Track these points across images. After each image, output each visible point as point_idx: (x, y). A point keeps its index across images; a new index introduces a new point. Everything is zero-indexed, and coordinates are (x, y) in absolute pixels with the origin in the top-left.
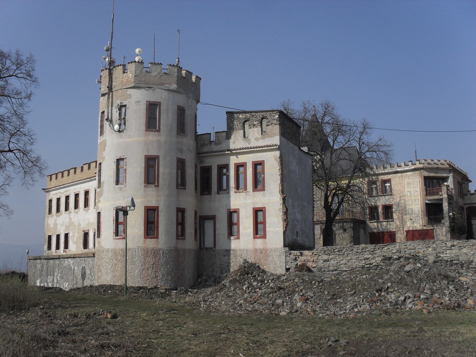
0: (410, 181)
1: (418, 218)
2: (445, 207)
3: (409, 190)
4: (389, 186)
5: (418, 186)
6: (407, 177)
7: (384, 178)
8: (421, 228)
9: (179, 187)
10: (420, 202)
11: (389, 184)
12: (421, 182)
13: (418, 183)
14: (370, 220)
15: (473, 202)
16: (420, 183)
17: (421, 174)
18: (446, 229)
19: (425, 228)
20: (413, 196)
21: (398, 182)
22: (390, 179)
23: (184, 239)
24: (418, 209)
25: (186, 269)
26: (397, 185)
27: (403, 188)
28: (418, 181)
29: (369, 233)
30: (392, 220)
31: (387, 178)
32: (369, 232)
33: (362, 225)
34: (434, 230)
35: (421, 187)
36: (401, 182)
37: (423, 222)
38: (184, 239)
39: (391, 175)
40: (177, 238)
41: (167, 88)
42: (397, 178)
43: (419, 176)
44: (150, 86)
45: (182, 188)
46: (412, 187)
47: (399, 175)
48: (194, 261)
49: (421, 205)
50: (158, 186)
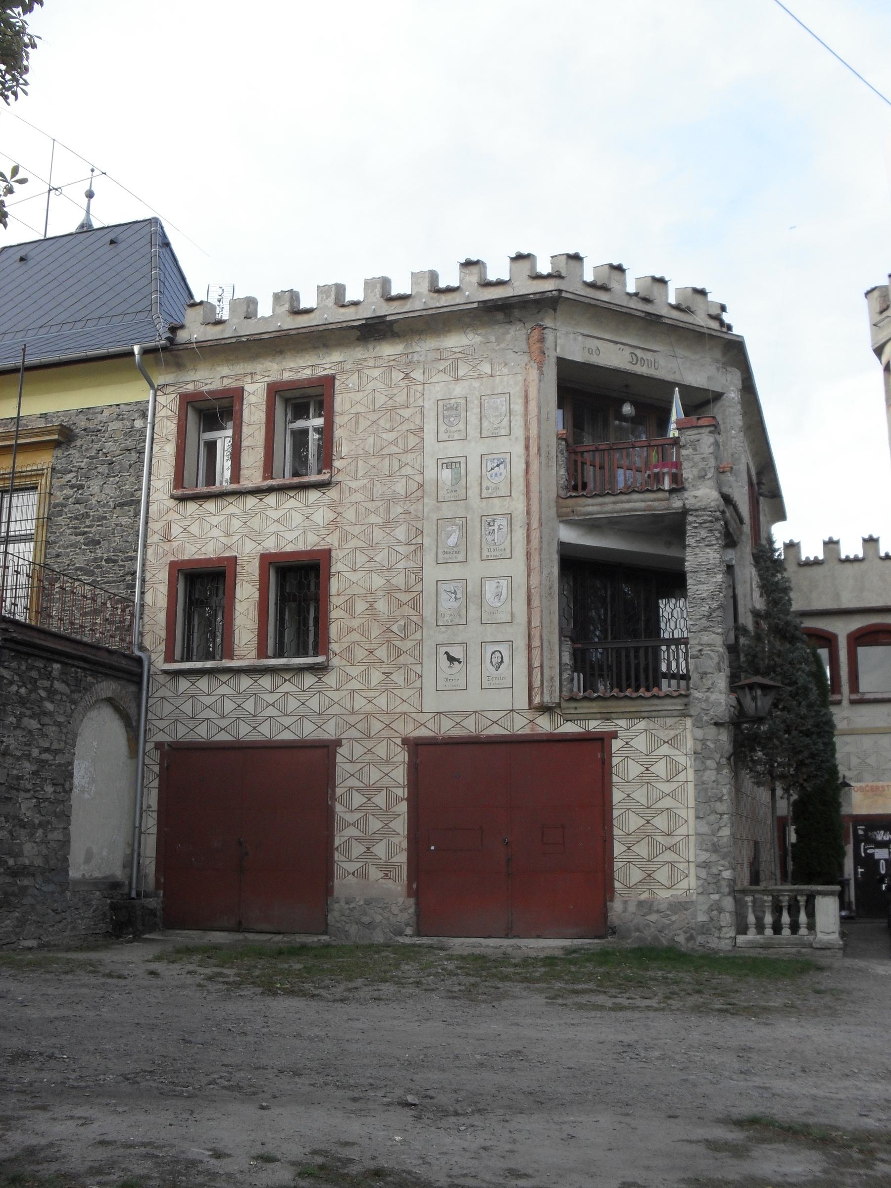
0: (459, 390)
1: (504, 649)
2: (703, 577)
3: (453, 450)
4: (317, 430)
5: (518, 422)
6: (442, 365)
7: (287, 376)
8: (520, 726)
10: (519, 535)
11: (319, 422)
12: (533, 393)
13: (518, 407)
15: (819, 604)
16: (533, 405)
17: (542, 340)
18: (699, 733)
19: (545, 725)
20: (473, 492)
21: (381, 400)
22: (330, 381)
24: (504, 583)
26: (373, 417)
27: (413, 441)
28: (516, 391)
29: (159, 746)
30: (321, 659)
31: (307, 373)
33: (107, 688)
34: (616, 744)
35: (534, 432)
36: (401, 399)
37: (537, 683)
39: (336, 356)
42: (376, 373)
43: (526, 358)
46: (473, 432)
47: (389, 350)
49: (528, 555)
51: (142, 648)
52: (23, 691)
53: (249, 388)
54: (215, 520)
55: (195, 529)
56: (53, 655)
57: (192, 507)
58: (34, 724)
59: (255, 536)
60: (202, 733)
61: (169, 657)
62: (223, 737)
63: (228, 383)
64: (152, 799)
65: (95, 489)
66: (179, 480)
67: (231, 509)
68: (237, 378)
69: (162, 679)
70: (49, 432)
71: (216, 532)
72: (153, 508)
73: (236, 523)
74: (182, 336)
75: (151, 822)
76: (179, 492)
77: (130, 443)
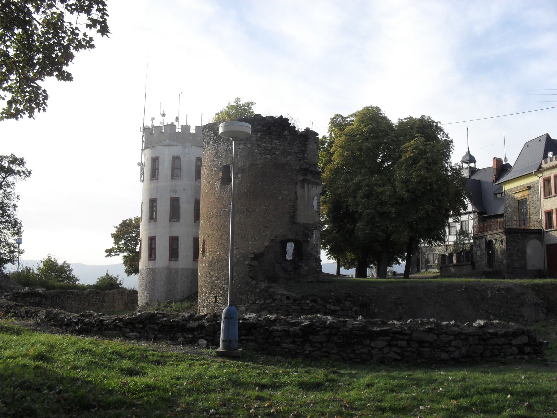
9: (172, 220)
14: (546, 229)
23: (177, 260)
25: (178, 284)
29: (546, 245)
32: (546, 244)
33: (533, 236)
38: (177, 260)
40: (170, 260)
41: (163, 144)
44: (153, 145)
45: (175, 220)
48: (191, 278)
50: (156, 221)
51: (542, 228)
52: (512, 239)
53: (551, 176)
54: (549, 202)
55: (547, 204)
56: (518, 233)
57: (546, 200)
58: (515, 244)
59: (554, 205)
60: (551, 242)
61: (546, 229)
62: (554, 243)
63: (549, 175)
64: (546, 254)
65: (534, 198)
66: (545, 195)
67: (551, 200)
68: (550, 174)
69: (545, 233)
70: (526, 188)
71: (550, 205)
72: (542, 201)
73: (552, 203)
74: (542, 166)
75: (546, 259)
76: (545, 198)
77: (538, 189)
